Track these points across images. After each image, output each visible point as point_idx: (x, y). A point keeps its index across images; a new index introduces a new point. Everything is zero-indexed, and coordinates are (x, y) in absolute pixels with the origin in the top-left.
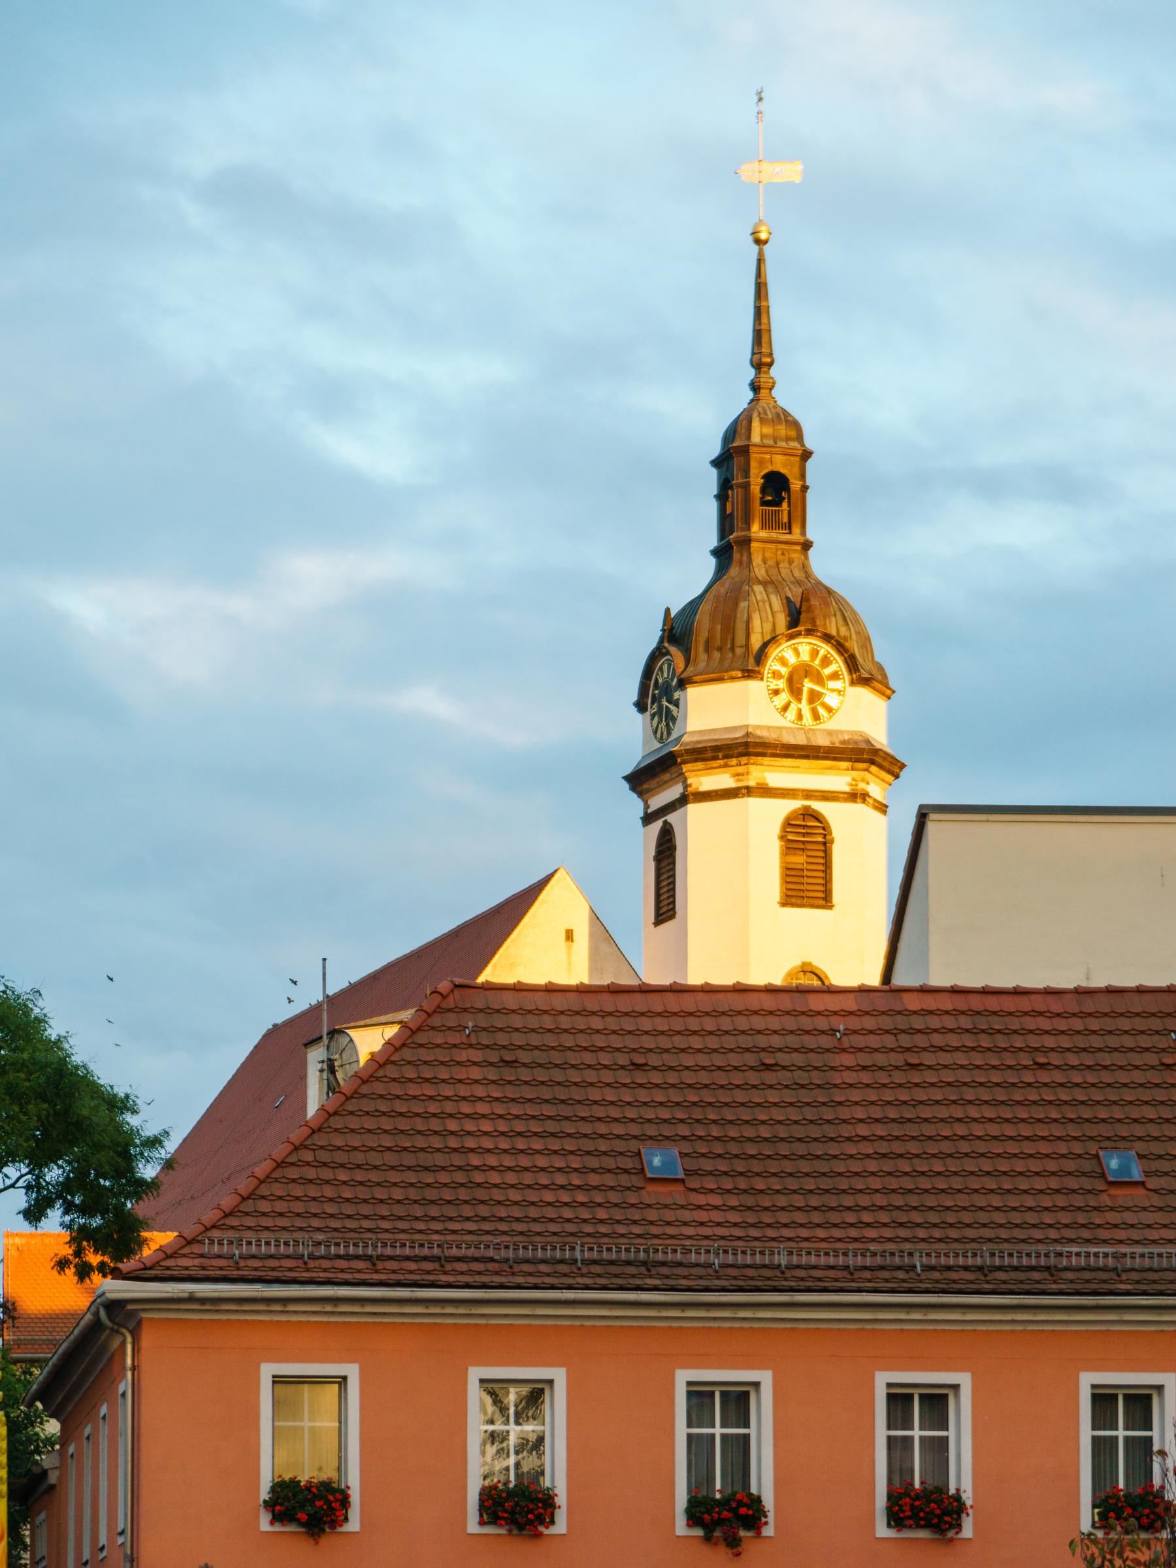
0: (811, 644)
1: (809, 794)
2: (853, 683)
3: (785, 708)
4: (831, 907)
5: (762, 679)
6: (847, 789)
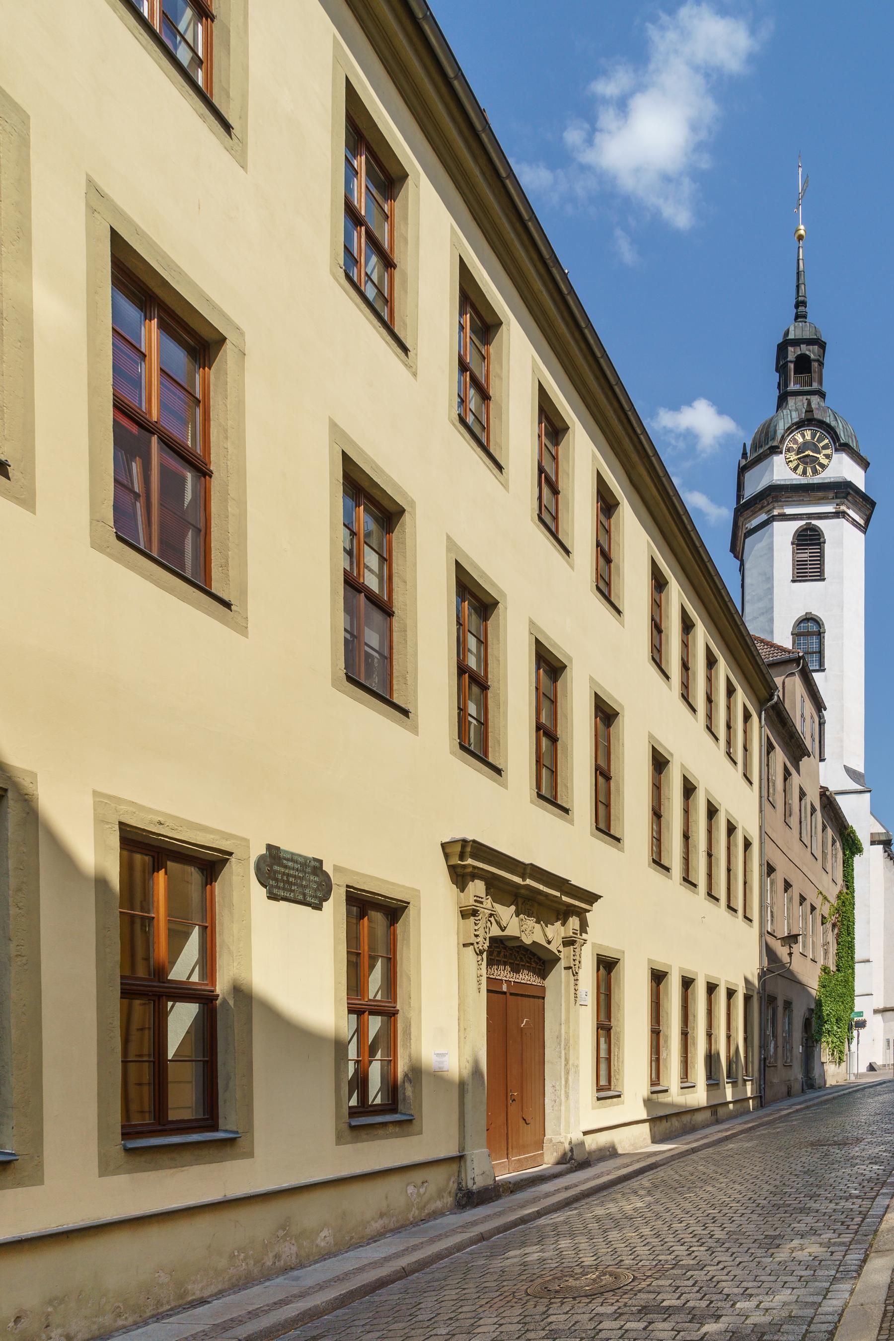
0: (811, 430)
1: (810, 516)
2: (836, 450)
3: (795, 469)
4: (824, 580)
5: (781, 453)
6: (834, 510)
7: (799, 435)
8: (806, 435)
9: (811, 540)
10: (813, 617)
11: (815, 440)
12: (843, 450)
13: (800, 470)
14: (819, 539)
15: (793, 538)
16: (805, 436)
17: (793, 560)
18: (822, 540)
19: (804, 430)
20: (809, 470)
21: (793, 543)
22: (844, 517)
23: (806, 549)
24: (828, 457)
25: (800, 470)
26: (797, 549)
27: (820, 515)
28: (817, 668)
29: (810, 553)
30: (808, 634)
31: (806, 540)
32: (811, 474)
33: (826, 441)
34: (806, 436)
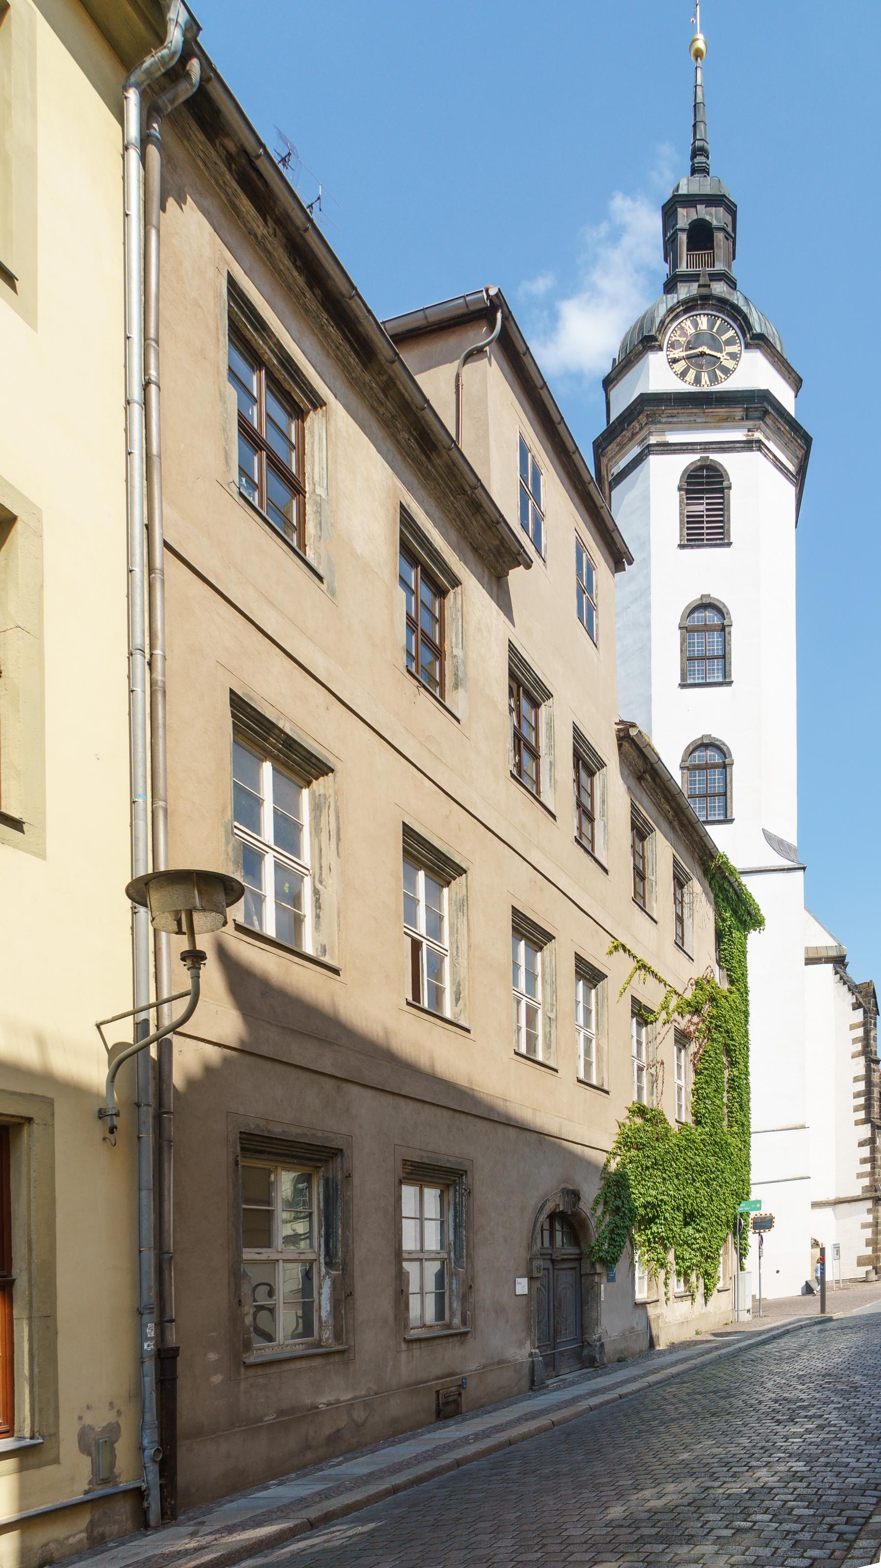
0: (708, 315)
1: (707, 446)
2: (747, 346)
3: (683, 375)
4: (729, 544)
7: (688, 323)
8: (700, 322)
9: (708, 484)
10: (712, 601)
11: (714, 330)
12: (758, 347)
14: (721, 483)
15: (681, 481)
16: (698, 324)
17: (681, 514)
18: (725, 484)
19: (696, 315)
20: (705, 378)
21: (680, 489)
22: (760, 449)
23: (702, 498)
24: (734, 356)
26: (688, 499)
27: (723, 446)
28: (721, 680)
29: (708, 504)
30: (706, 629)
31: (702, 484)
32: (708, 383)
33: (731, 333)
34: (700, 325)
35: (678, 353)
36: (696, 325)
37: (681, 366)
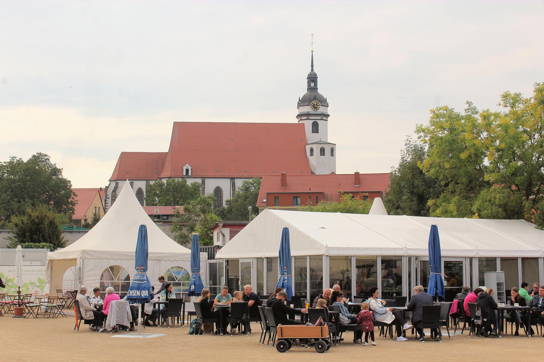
3: (312, 109)
4: (318, 133)
13: (313, 109)
20: (315, 110)
24: (319, 107)
25: (313, 109)
33: (319, 104)
35: (312, 106)
36: (314, 103)
37: (312, 108)
